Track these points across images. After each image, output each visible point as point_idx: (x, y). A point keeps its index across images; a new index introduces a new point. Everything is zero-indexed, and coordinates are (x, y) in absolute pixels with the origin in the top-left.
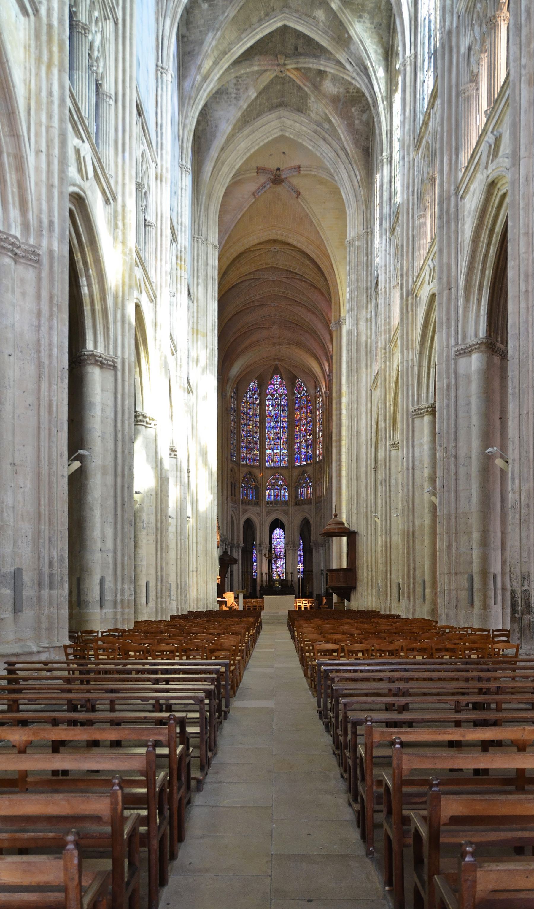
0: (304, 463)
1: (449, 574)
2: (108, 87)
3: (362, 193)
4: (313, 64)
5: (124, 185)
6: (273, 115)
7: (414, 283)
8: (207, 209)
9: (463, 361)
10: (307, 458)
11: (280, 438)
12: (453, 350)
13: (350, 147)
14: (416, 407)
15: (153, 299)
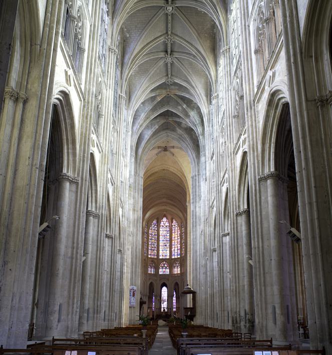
0: (176, 257)
1: (221, 311)
3: (196, 160)
9: (224, 238)
10: (178, 255)
11: (166, 246)
13: (191, 144)
14: (213, 248)
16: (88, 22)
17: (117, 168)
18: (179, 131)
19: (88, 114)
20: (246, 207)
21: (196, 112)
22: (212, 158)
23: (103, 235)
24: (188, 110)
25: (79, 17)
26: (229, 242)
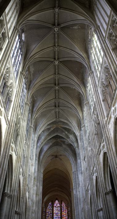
2: (25, 156)
3: (75, 162)
4: (63, 140)
5: (26, 172)
6: (55, 147)
7: (87, 189)
8: (41, 165)
12: (96, 210)
15: (29, 192)
16: (15, 89)
17: (27, 166)
18: (64, 146)
19: (10, 132)
20: (111, 188)
21: (73, 135)
22: (84, 159)
23: (13, 212)
24: (69, 134)
25: (11, 87)
26: (103, 216)
